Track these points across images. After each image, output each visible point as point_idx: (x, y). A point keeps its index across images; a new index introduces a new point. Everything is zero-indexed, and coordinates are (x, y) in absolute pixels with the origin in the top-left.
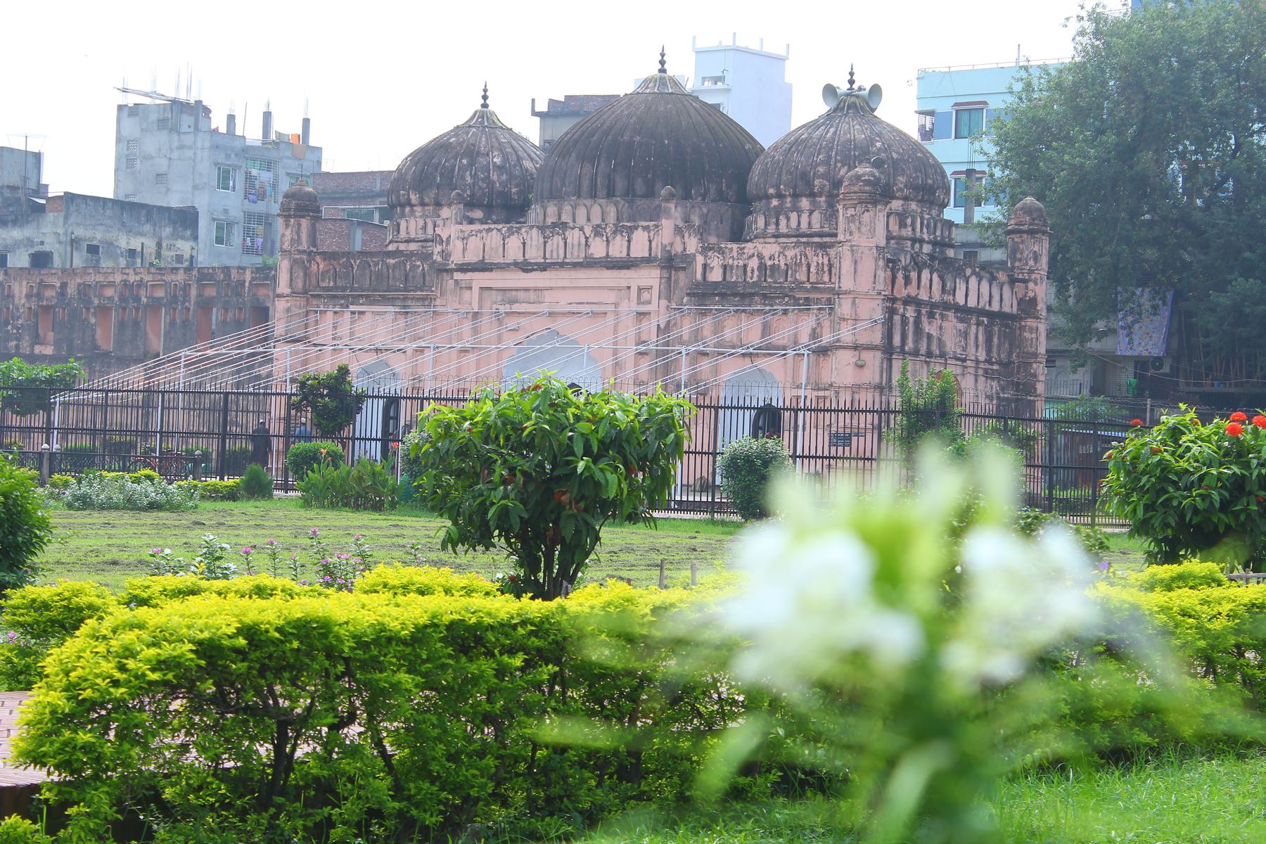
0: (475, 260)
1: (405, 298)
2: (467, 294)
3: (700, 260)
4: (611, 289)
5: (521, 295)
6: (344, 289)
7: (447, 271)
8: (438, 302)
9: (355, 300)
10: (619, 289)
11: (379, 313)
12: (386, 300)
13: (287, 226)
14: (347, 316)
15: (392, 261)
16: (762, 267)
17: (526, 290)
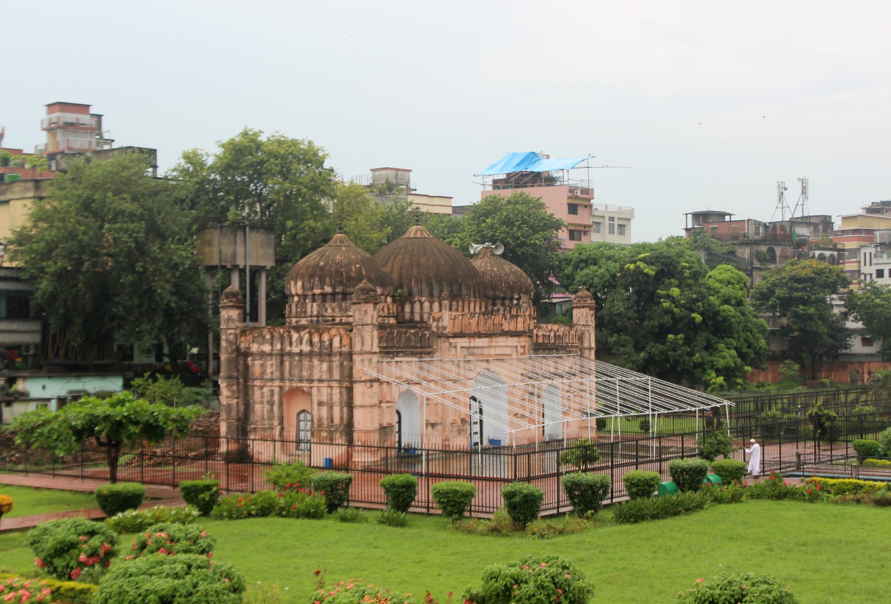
0: (458, 331)
1: (421, 353)
2: (453, 350)
3: (535, 331)
4: (509, 347)
5: (476, 351)
6: (392, 347)
7: (440, 337)
8: (436, 354)
9: (397, 354)
10: (512, 347)
11: (407, 362)
12: (413, 354)
13: (374, 309)
14: (394, 364)
15: (413, 331)
16: (555, 336)
17: (478, 347)
